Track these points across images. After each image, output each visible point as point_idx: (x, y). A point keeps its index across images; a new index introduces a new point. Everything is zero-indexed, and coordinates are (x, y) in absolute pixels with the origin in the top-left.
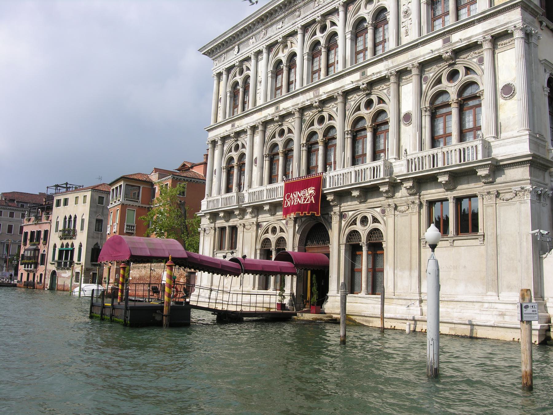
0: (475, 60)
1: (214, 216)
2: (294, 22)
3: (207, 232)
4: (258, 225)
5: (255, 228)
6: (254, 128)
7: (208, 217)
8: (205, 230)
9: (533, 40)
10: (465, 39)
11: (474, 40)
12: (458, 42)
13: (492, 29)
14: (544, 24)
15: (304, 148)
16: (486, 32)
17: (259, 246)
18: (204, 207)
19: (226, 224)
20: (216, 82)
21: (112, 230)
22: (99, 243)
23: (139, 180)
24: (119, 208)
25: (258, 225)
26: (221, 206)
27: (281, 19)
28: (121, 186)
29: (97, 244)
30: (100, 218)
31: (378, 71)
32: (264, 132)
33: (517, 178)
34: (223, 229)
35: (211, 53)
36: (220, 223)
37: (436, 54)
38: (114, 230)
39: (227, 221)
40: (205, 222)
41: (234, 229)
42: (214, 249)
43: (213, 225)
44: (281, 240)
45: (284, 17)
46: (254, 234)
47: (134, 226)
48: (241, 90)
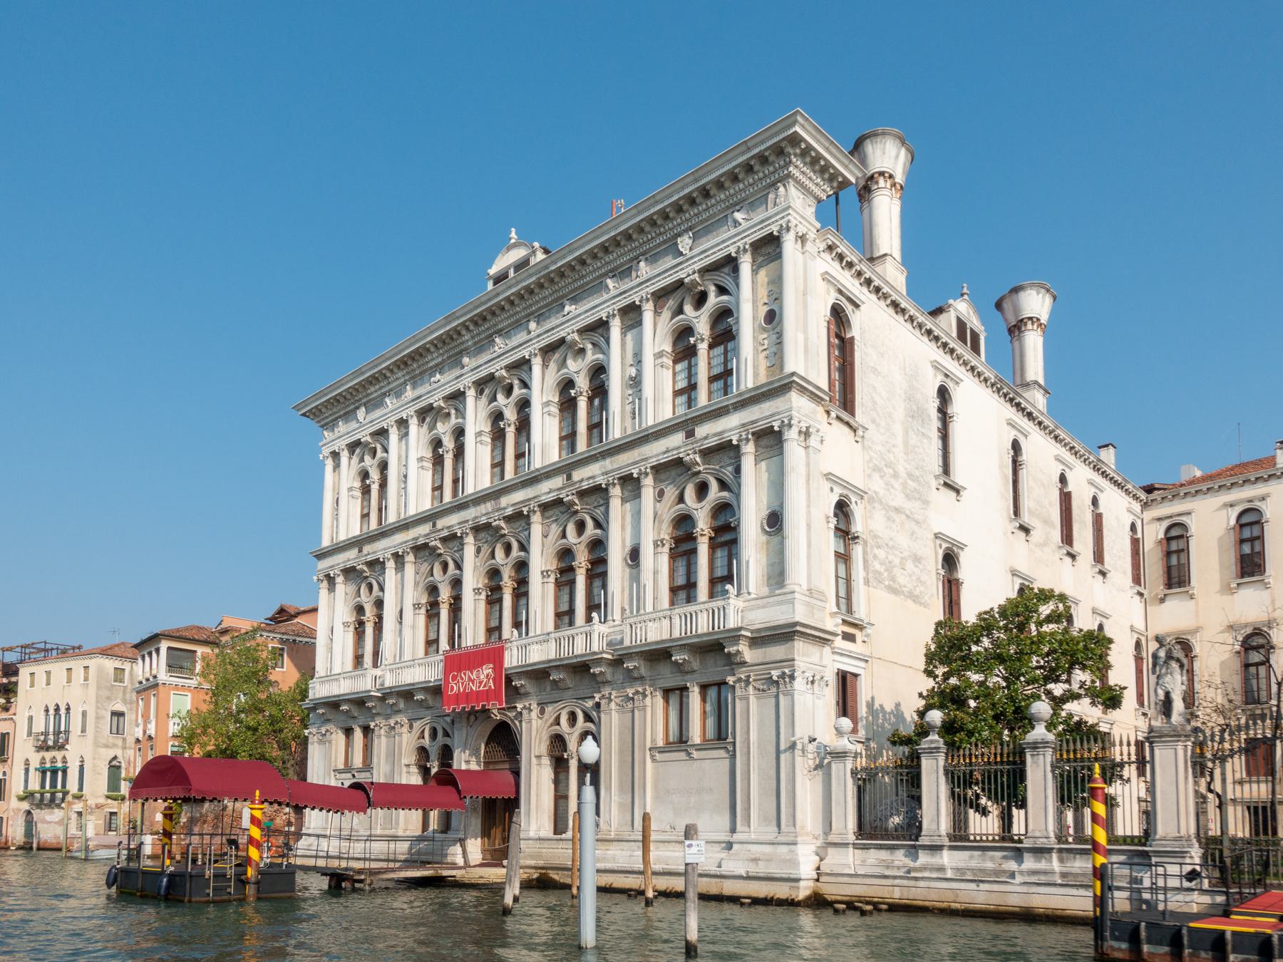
0: (730, 469)
9: (813, 441)
10: (715, 435)
11: (726, 437)
12: (706, 438)
13: (753, 422)
14: (833, 415)
16: (743, 425)
31: (590, 474)
33: (779, 658)
35: (314, 414)
37: (672, 456)
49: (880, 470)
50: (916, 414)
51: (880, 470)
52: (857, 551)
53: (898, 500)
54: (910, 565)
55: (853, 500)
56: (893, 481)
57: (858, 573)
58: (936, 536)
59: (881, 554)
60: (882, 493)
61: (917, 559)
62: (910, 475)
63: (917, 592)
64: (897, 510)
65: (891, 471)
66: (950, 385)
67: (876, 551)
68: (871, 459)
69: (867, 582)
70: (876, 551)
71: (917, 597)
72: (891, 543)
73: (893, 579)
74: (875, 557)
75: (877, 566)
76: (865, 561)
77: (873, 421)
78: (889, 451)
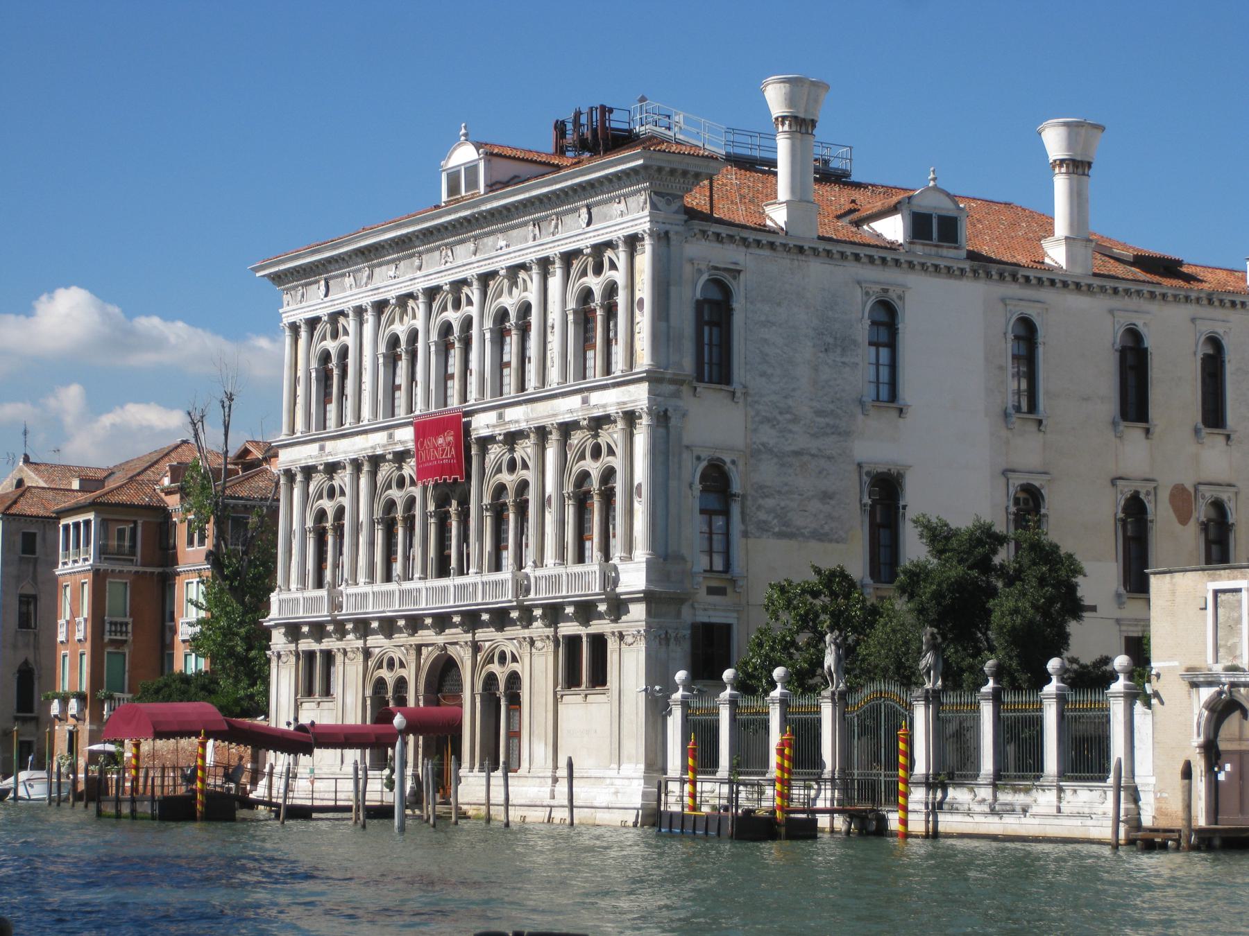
1: (293, 631)
2: (411, 276)
3: (284, 659)
4: (367, 653)
5: (361, 657)
6: (357, 465)
7: (283, 630)
8: (279, 656)
9: (673, 422)
15: (433, 520)
16: (618, 404)
17: (369, 692)
18: (274, 612)
19: (315, 646)
20: (288, 341)
21: (71, 632)
22: (31, 659)
23: (132, 506)
24: (88, 580)
25: (367, 653)
26: (301, 614)
27: (393, 261)
28: (87, 523)
29: (26, 662)
30: (28, 590)
32: (374, 474)
34: (310, 655)
36: (306, 645)
38: (79, 635)
39: (319, 641)
40: (278, 640)
41: (329, 657)
42: (296, 695)
43: (292, 647)
44: (401, 683)
45: (399, 259)
46: (361, 668)
47: (127, 624)
48: (335, 372)
49: (768, 420)
50: (833, 343)
51: (768, 420)
52: (736, 510)
53: (801, 441)
54: (815, 506)
55: (728, 460)
56: (790, 426)
57: (737, 526)
58: (860, 466)
59: (770, 503)
60: (772, 442)
61: (826, 496)
62: (819, 413)
63: (827, 528)
64: (797, 454)
65: (788, 416)
66: (892, 296)
67: (761, 501)
68: (758, 413)
69: (745, 534)
70: (761, 501)
71: (826, 534)
72: (786, 488)
73: (787, 524)
74: (759, 508)
75: (762, 516)
76: (743, 513)
77: (763, 374)
78: (786, 397)
